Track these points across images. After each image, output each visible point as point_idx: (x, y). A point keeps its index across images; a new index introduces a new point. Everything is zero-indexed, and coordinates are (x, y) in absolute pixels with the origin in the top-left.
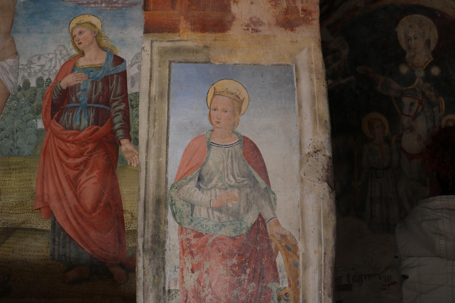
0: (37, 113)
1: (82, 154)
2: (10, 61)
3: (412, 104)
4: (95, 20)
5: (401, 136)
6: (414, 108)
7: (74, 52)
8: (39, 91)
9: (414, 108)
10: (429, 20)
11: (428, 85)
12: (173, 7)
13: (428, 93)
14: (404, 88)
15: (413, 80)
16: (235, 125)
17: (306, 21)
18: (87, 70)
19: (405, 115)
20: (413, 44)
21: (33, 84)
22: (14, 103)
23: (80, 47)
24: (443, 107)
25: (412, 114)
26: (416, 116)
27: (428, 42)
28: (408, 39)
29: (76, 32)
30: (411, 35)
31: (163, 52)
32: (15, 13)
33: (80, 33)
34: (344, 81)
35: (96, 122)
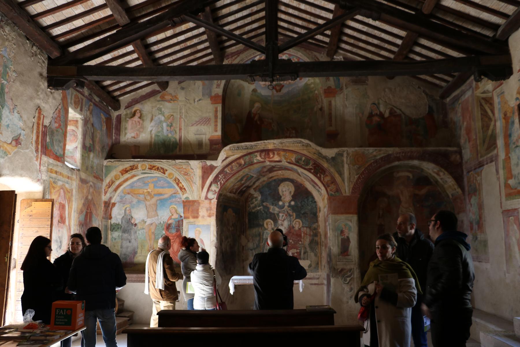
0: (163, 229)
1: (173, 239)
2: (156, 217)
3: (283, 216)
4: (175, 206)
6: (284, 217)
7: (171, 215)
8: (163, 224)
9: (284, 217)
11: (290, 208)
12: (189, 213)
13: (289, 211)
16: (199, 236)
17: (213, 215)
18: (174, 219)
21: (162, 223)
22: (158, 227)
23: (172, 213)
24: (295, 216)
25: (283, 219)
26: (284, 220)
27: (290, 192)
28: (283, 192)
29: (171, 210)
30: (284, 190)
31: (187, 223)
32: (157, 205)
33: (172, 210)
34: (259, 208)
35: (177, 232)
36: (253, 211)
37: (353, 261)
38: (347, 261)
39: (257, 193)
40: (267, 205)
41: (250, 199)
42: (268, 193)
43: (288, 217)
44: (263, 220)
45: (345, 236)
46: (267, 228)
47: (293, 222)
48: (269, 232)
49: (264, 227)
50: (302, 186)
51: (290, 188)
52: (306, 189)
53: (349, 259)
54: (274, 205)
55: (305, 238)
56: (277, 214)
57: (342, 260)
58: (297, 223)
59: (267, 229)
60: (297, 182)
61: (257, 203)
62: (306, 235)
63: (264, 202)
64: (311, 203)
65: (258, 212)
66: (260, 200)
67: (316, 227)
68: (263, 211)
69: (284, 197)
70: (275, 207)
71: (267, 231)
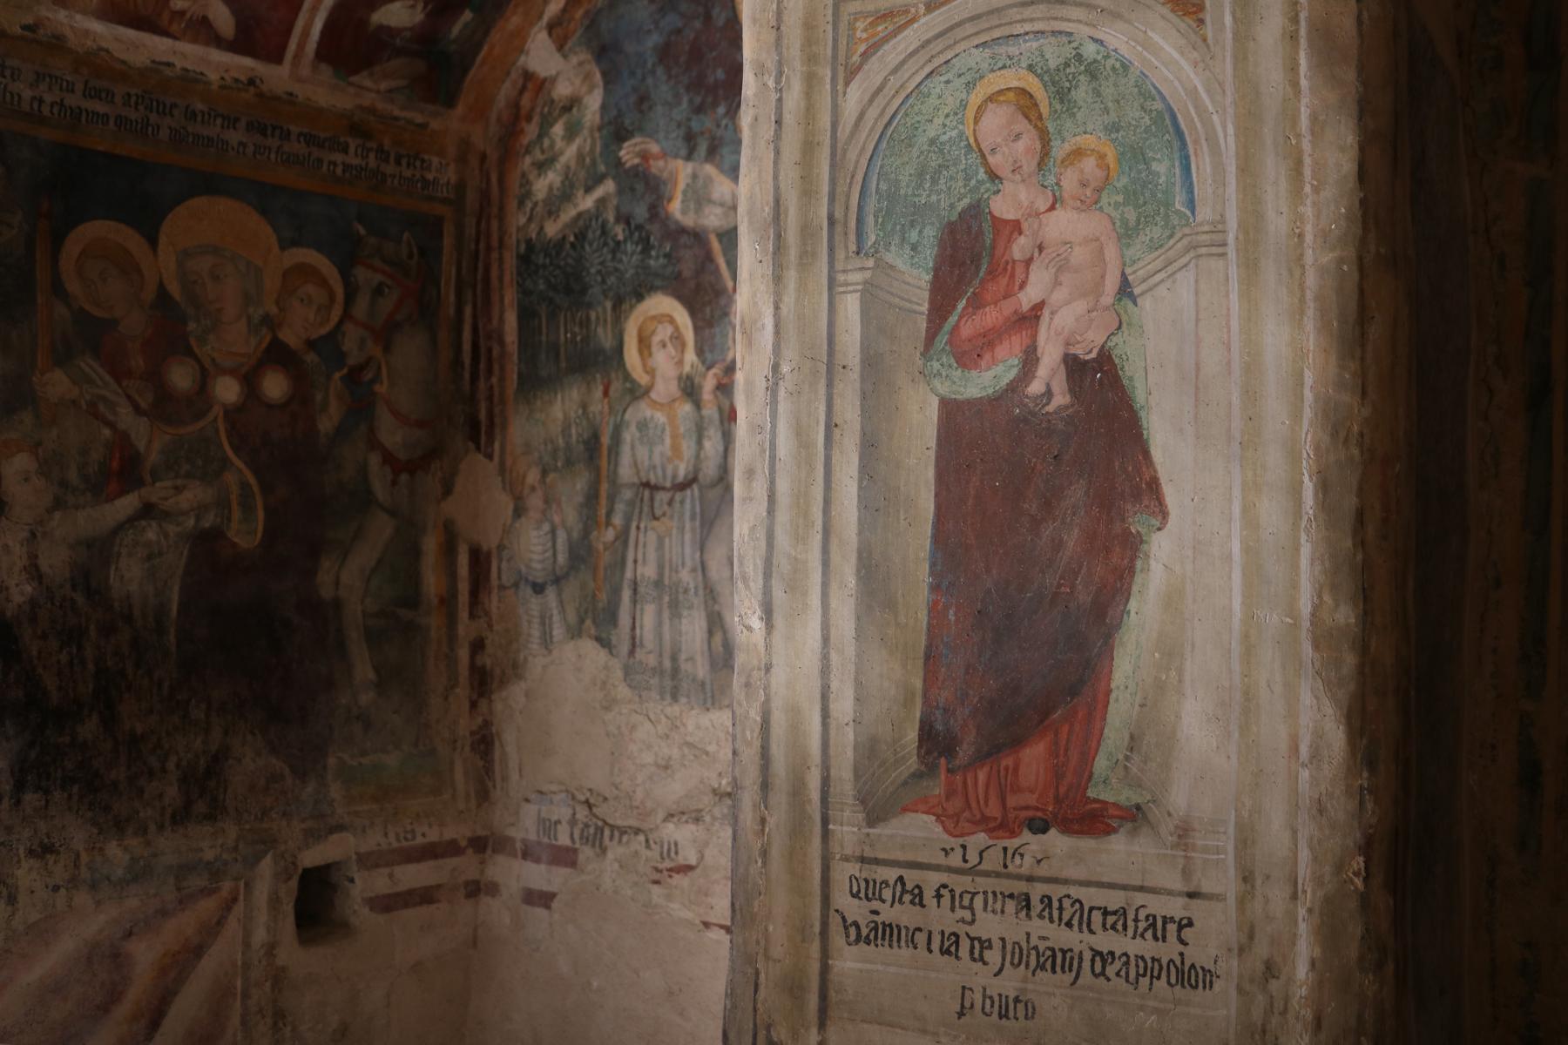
34: (587, 203)
36: (552, 229)
37: (1190, 976)
38: (1058, 960)
39: (574, 60)
41: (531, 130)
42: (655, 39)
44: (618, 303)
45: (1030, 360)
48: (660, 417)
49: (627, 377)
53: (1116, 919)
54: (703, 148)
57: (941, 918)
59: (647, 391)
66: (597, 118)
70: (709, 169)
71: (643, 410)
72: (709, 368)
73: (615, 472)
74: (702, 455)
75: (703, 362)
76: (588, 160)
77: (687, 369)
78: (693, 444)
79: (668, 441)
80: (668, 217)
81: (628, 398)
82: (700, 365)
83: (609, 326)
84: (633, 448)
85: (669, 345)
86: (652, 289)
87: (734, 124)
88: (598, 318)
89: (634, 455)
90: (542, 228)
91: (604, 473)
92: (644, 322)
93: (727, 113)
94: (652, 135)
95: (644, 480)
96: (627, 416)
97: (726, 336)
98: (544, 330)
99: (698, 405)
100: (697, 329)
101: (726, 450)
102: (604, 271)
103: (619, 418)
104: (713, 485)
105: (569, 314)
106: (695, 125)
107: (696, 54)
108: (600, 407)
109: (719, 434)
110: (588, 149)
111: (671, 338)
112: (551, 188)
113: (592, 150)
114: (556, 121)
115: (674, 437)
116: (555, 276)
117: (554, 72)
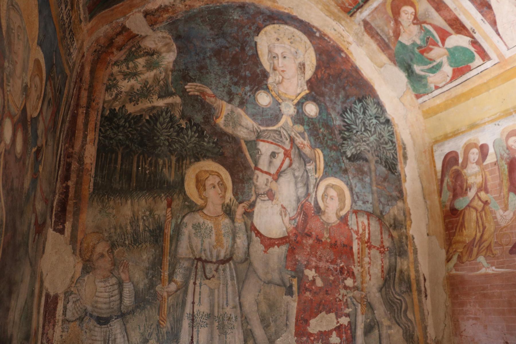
3: (273, 155)
5: (252, 205)
6: (277, 162)
9: (277, 162)
10: (305, 38)
11: (300, 128)
13: (299, 140)
14: (262, 128)
15: (277, 118)
19: (262, 171)
20: (280, 65)
24: (321, 165)
25: (273, 171)
26: (279, 174)
27: (302, 67)
30: (278, 51)
34: (161, 103)
36: (131, 109)
40: (203, 93)
43: (295, 165)
44: (181, 159)
46: (200, 202)
47: (317, 186)
48: (209, 224)
49: (186, 198)
50: (343, 55)
51: (301, 51)
52: (356, 70)
54: (237, 100)
55: (367, 259)
56: (247, 142)
58: (333, 193)
59: (201, 209)
60: (323, 37)
61: (156, 79)
62: (370, 248)
63: (194, 81)
64: (374, 121)
65: (155, 119)
66: (171, 66)
67: (401, 218)
68: (183, 117)
69: (278, 78)
70: (239, 110)
71: (198, 218)
72: (240, 203)
73: (176, 250)
74: (235, 246)
75: (237, 200)
76: (162, 82)
77: (227, 201)
78: (230, 240)
79: (214, 237)
80: (215, 125)
81: (186, 211)
82: (235, 200)
83: (173, 169)
84: (189, 237)
85: (217, 186)
86: (205, 157)
87: (254, 96)
88: (164, 163)
89: (190, 242)
90: (124, 106)
91: (167, 250)
92: (200, 172)
93: (251, 91)
94: (209, 85)
95: (197, 257)
96: (185, 220)
97: (251, 189)
98: (119, 162)
99: (233, 220)
100: (233, 182)
101: (249, 245)
102: (170, 140)
103: (179, 221)
104: (242, 262)
105: (141, 157)
106: (233, 89)
107: (235, 60)
108: (164, 212)
109: (245, 237)
110: (162, 77)
111: (218, 184)
112: (132, 88)
113: (166, 79)
114: (140, 57)
115: (218, 235)
116: (132, 134)
117: (143, 34)
